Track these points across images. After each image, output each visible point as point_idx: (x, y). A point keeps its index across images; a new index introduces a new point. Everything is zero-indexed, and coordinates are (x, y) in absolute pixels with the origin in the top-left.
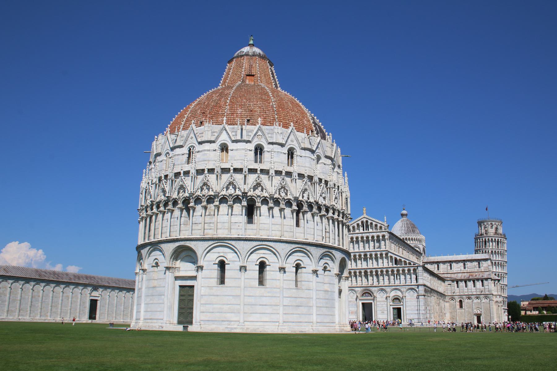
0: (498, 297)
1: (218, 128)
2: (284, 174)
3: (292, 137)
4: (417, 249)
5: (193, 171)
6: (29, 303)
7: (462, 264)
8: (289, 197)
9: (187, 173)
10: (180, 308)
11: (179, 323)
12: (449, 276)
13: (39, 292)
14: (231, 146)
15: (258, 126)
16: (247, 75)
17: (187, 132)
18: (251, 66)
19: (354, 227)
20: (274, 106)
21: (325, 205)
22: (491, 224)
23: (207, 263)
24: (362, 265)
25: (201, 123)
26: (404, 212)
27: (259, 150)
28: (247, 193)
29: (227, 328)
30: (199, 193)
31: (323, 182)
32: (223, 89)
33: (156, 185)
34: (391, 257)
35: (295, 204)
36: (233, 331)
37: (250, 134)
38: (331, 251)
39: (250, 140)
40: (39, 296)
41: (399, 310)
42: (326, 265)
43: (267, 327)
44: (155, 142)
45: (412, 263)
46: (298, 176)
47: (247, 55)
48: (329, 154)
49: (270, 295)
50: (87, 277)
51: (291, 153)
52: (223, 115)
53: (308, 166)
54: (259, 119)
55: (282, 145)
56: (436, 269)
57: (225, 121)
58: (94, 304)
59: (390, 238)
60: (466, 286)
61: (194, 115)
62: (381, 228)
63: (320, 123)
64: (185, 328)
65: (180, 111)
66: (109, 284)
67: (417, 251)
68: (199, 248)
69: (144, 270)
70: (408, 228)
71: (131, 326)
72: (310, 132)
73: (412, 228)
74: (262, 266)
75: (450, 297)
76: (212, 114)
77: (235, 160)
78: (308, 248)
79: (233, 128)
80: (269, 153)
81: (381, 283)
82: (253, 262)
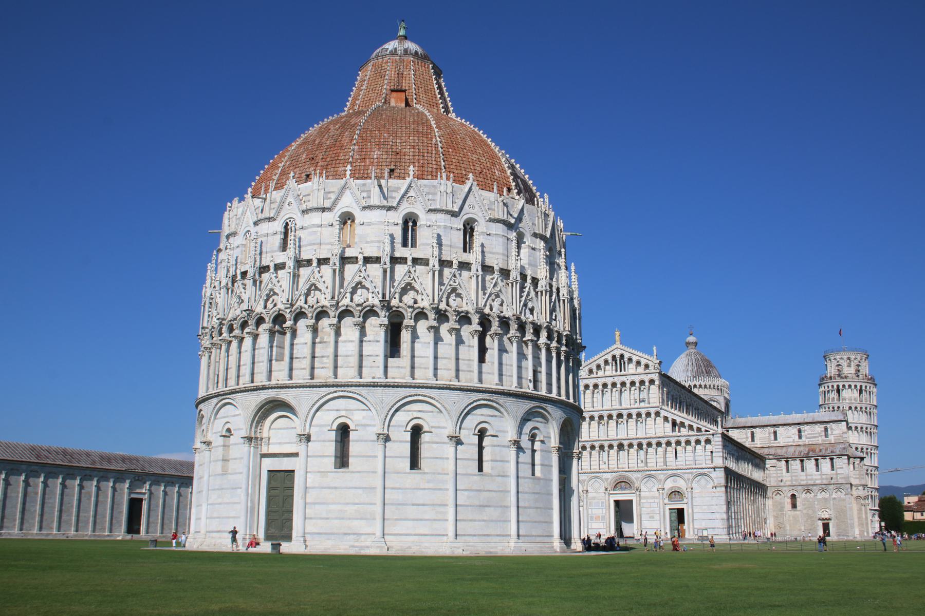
0: (861, 488)
1: (335, 185)
2: (455, 266)
3: (471, 199)
4: (715, 404)
5: (290, 264)
6: (19, 506)
7: (794, 430)
8: (465, 308)
9: (279, 267)
11: (268, 538)
12: (772, 451)
13: (38, 486)
14: (359, 216)
15: (408, 180)
16: (393, 91)
17: (281, 192)
18: (400, 75)
19: (598, 367)
20: (440, 145)
21: (533, 323)
22: (849, 359)
24: (613, 432)
25: (308, 176)
26: (692, 339)
27: (410, 223)
28: (389, 302)
29: (353, 546)
30: (301, 303)
31: (529, 280)
32: (349, 116)
33: (228, 290)
34: (666, 419)
37: (394, 194)
38: (544, 405)
39: (395, 205)
40: (37, 494)
41: (680, 512)
42: (536, 431)
43: (426, 544)
44: (226, 213)
45: (703, 429)
46: (483, 270)
47: (394, 52)
48: (540, 231)
49: (431, 485)
50: (124, 459)
51: (469, 229)
52: (346, 162)
53: (501, 251)
54: (411, 168)
55: (454, 214)
56: (750, 439)
57: (348, 173)
58: (135, 506)
60: (803, 470)
61: (294, 163)
62: (647, 366)
63: (527, 176)
64: (276, 546)
65: (273, 158)
66: (164, 470)
67: (715, 408)
69: (208, 443)
70: (698, 366)
71: (187, 545)
72: (505, 190)
73: (705, 368)
74: (416, 432)
75: (773, 489)
77: (367, 242)
78: (502, 400)
79: (364, 185)
81: (652, 465)
82: (399, 426)
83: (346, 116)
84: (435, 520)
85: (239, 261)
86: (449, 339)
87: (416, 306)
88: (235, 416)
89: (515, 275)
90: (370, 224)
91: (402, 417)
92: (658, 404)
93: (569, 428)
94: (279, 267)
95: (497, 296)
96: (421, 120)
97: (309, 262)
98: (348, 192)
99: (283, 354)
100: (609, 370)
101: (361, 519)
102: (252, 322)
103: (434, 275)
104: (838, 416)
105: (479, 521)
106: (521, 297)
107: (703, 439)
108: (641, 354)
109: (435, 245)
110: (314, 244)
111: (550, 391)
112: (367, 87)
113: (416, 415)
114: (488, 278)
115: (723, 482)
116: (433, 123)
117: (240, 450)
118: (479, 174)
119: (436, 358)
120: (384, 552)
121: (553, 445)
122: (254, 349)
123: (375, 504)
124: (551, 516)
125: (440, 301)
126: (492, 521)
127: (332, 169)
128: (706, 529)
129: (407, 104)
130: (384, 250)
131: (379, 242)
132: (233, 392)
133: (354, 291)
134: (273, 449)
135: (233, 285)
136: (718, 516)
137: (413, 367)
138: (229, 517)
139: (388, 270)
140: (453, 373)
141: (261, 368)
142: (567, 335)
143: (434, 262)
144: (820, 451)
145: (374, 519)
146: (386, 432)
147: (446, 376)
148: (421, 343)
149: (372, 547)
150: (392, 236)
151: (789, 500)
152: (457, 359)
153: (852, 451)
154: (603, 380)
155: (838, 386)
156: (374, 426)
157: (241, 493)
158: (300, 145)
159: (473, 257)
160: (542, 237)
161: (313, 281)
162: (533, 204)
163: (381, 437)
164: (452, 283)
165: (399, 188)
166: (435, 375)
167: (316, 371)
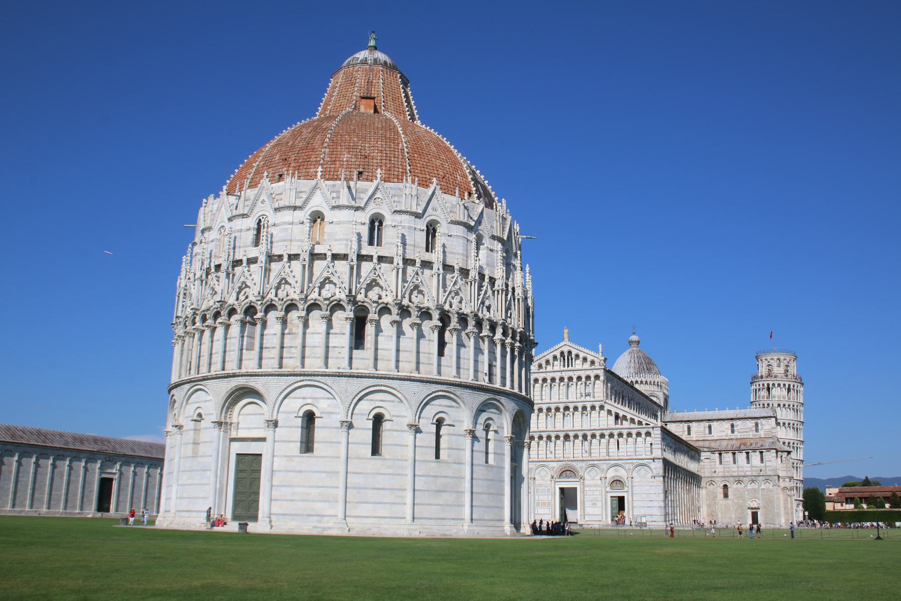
0: (787, 480)
1: (306, 185)
2: (418, 265)
3: (434, 202)
4: (654, 399)
5: (262, 258)
7: (727, 425)
8: (426, 304)
9: (252, 261)
10: (236, 493)
11: (235, 517)
12: (707, 444)
14: (329, 215)
15: (375, 183)
16: (362, 98)
17: (255, 191)
18: (370, 83)
19: (548, 362)
21: (489, 320)
22: (779, 359)
23: (284, 416)
24: (560, 424)
25: (281, 176)
26: (634, 338)
27: (376, 223)
28: (355, 297)
29: (316, 527)
30: (271, 296)
31: (487, 280)
32: (321, 120)
33: (202, 281)
34: (609, 412)
35: (437, 316)
36: (326, 533)
37: (362, 196)
38: (498, 397)
39: (362, 205)
41: (621, 500)
42: (490, 422)
43: (385, 526)
44: (202, 209)
45: (644, 422)
47: (364, 62)
48: (498, 234)
49: (390, 471)
51: (431, 230)
52: (317, 163)
53: (461, 252)
54: (379, 171)
55: (418, 216)
57: (319, 174)
59: (607, 380)
60: (734, 462)
62: (593, 363)
63: (486, 182)
64: (243, 526)
65: (247, 158)
67: (655, 403)
68: (270, 387)
69: (180, 427)
70: (640, 364)
71: (157, 523)
72: (466, 194)
73: (647, 365)
74: (378, 420)
76: (298, 162)
77: (336, 240)
78: (459, 391)
79: (334, 186)
80: (395, 229)
81: (595, 455)
82: (362, 414)
83: (318, 120)
84: (394, 503)
85: (213, 254)
86: (410, 333)
87: (380, 301)
88: (206, 401)
89: (473, 274)
90: (339, 223)
91: (365, 406)
92: (602, 398)
93: (521, 419)
94: (252, 261)
95: (457, 294)
96: (389, 126)
97: (280, 257)
98: (318, 192)
99: (253, 344)
100: (558, 366)
101: (325, 501)
102: (224, 313)
103: (398, 272)
104: (767, 412)
105: (435, 505)
106: (479, 295)
107: (643, 432)
108: (587, 351)
109: (399, 244)
110: (285, 240)
111: (504, 384)
112: (339, 93)
113: (378, 404)
114: (449, 276)
115: (661, 472)
116: (400, 129)
117: (210, 435)
118: (442, 179)
119: (398, 350)
120: (345, 533)
121: (506, 435)
122: (226, 339)
123: (337, 487)
124: (502, 502)
125: (403, 297)
126: (448, 505)
127: (303, 169)
128: (645, 516)
129: (376, 111)
130: (351, 248)
131: (347, 240)
132: (205, 379)
133: (322, 286)
134: (242, 434)
135: (207, 277)
136: (656, 504)
137: (376, 359)
138: (198, 498)
139: (355, 267)
140: (414, 365)
141: (233, 356)
142: (520, 332)
143: (398, 260)
144: (751, 444)
145: (337, 502)
146: (349, 419)
147: (407, 368)
148: (384, 336)
149: (333, 527)
150: (359, 235)
151: (722, 490)
152: (418, 352)
153: (780, 446)
154: (552, 375)
155: (768, 385)
156: (339, 413)
157: (211, 475)
158: (274, 147)
159: (435, 257)
160: (500, 240)
161: (283, 275)
162: (492, 208)
163: (345, 424)
164: (414, 280)
165: (367, 190)
166: (397, 367)
167: (285, 361)
